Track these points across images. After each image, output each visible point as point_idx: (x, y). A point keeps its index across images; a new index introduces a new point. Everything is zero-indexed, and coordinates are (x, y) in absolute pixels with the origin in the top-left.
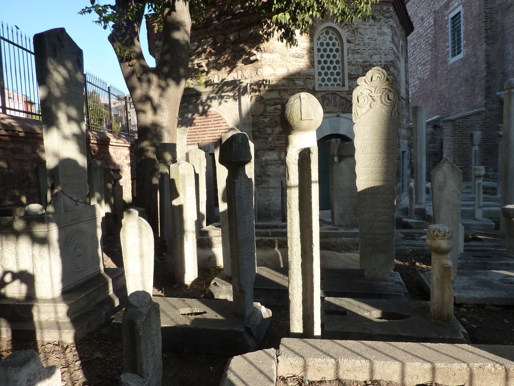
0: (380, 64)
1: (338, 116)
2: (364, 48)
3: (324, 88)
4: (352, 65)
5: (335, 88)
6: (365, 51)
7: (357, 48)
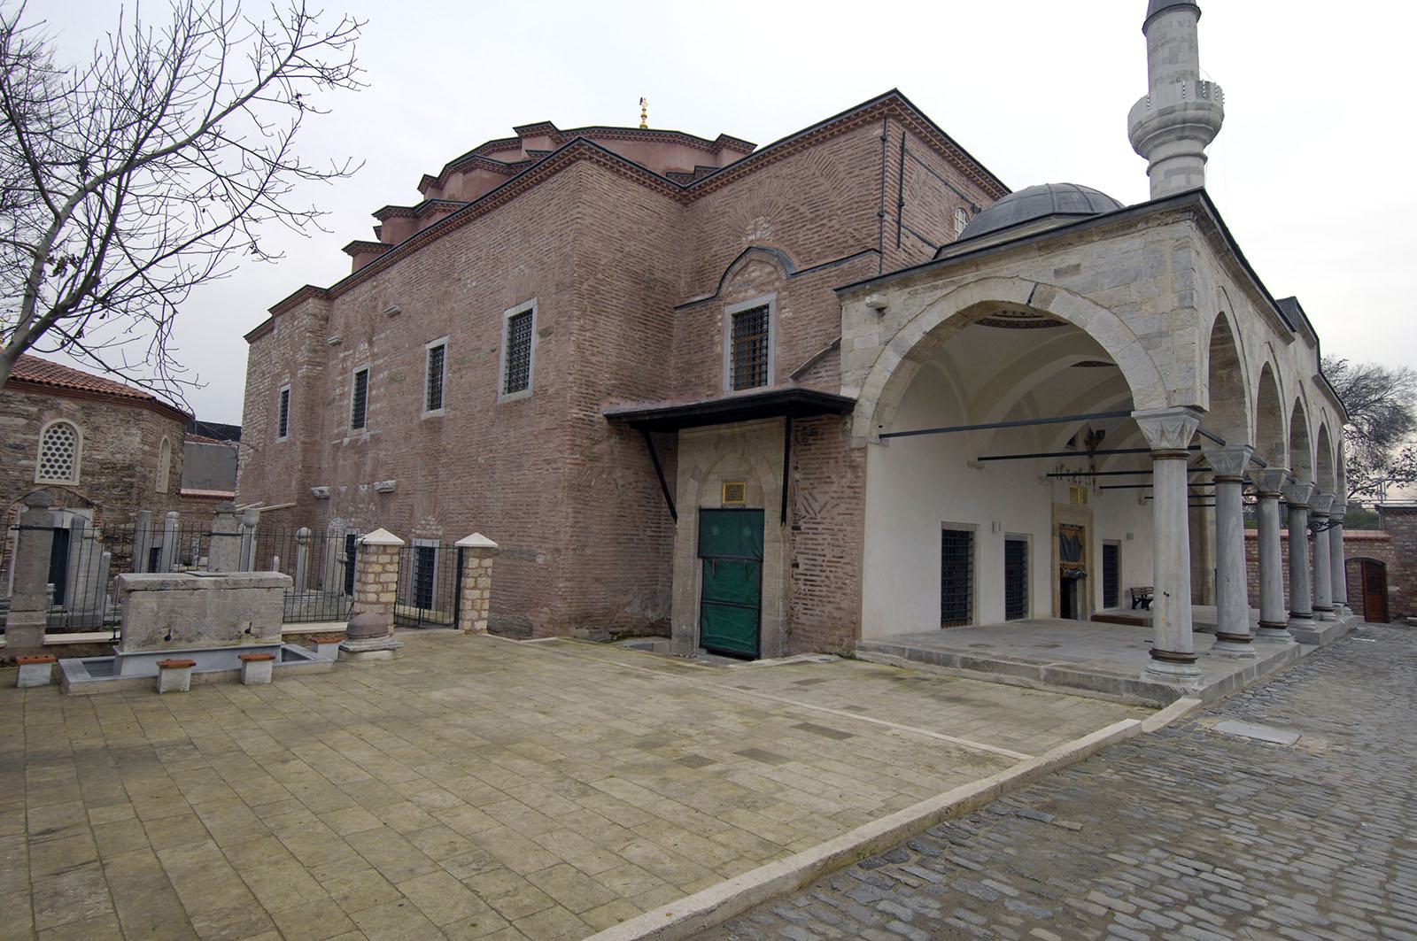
1: (61, 510)
3: (47, 481)
5: (63, 482)
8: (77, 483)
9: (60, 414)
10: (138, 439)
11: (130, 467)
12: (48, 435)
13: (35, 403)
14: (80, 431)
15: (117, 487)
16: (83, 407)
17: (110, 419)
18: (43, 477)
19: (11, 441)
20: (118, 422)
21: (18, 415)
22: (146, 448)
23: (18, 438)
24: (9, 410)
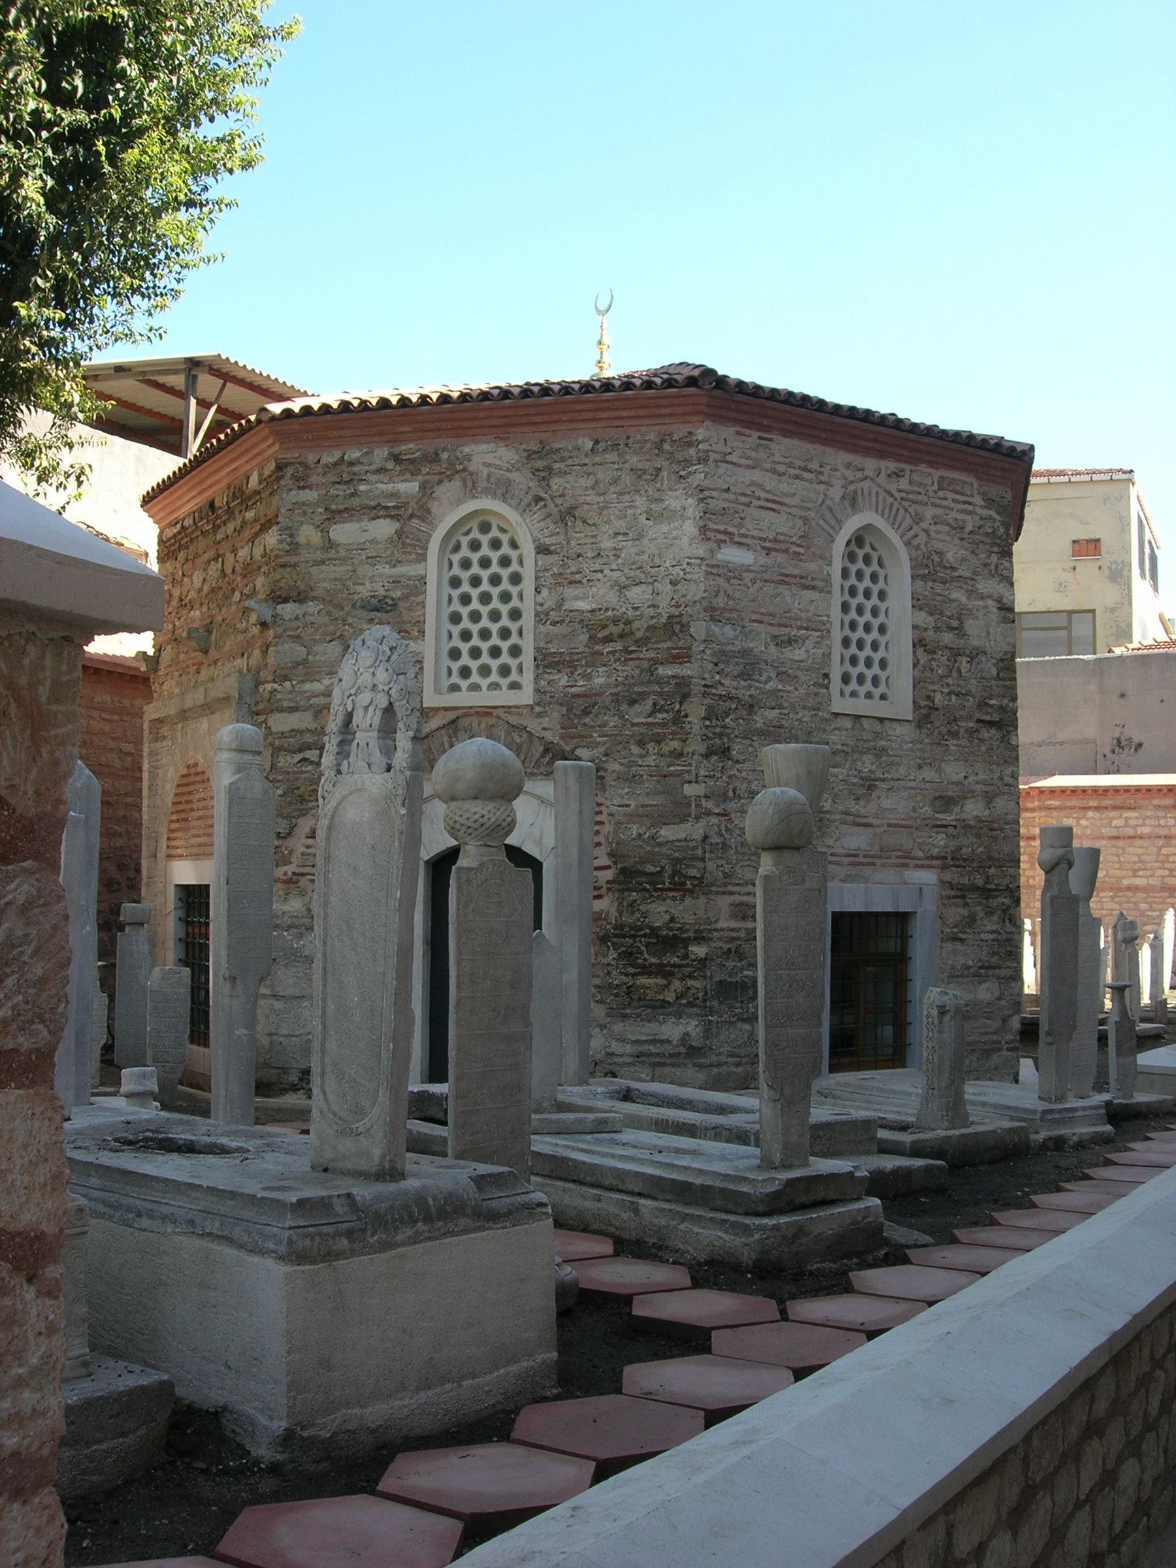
0: (651, 611)
2: (597, 567)
4: (554, 623)
6: (599, 575)
7: (573, 569)
8: (526, 696)
9: (472, 488)
10: (690, 528)
11: (675, 626)
12: (456, 558)
13: (407, 465)
14: (524, 528)
15: (643, 695)
16: (530, 455)
17: (603, 475)
18: (455, 688)
19: (364, 591)
20: (627, 479)
21: (376, 511)
22: (732, 555)
23: (374, 581)
24: (356, 502)
